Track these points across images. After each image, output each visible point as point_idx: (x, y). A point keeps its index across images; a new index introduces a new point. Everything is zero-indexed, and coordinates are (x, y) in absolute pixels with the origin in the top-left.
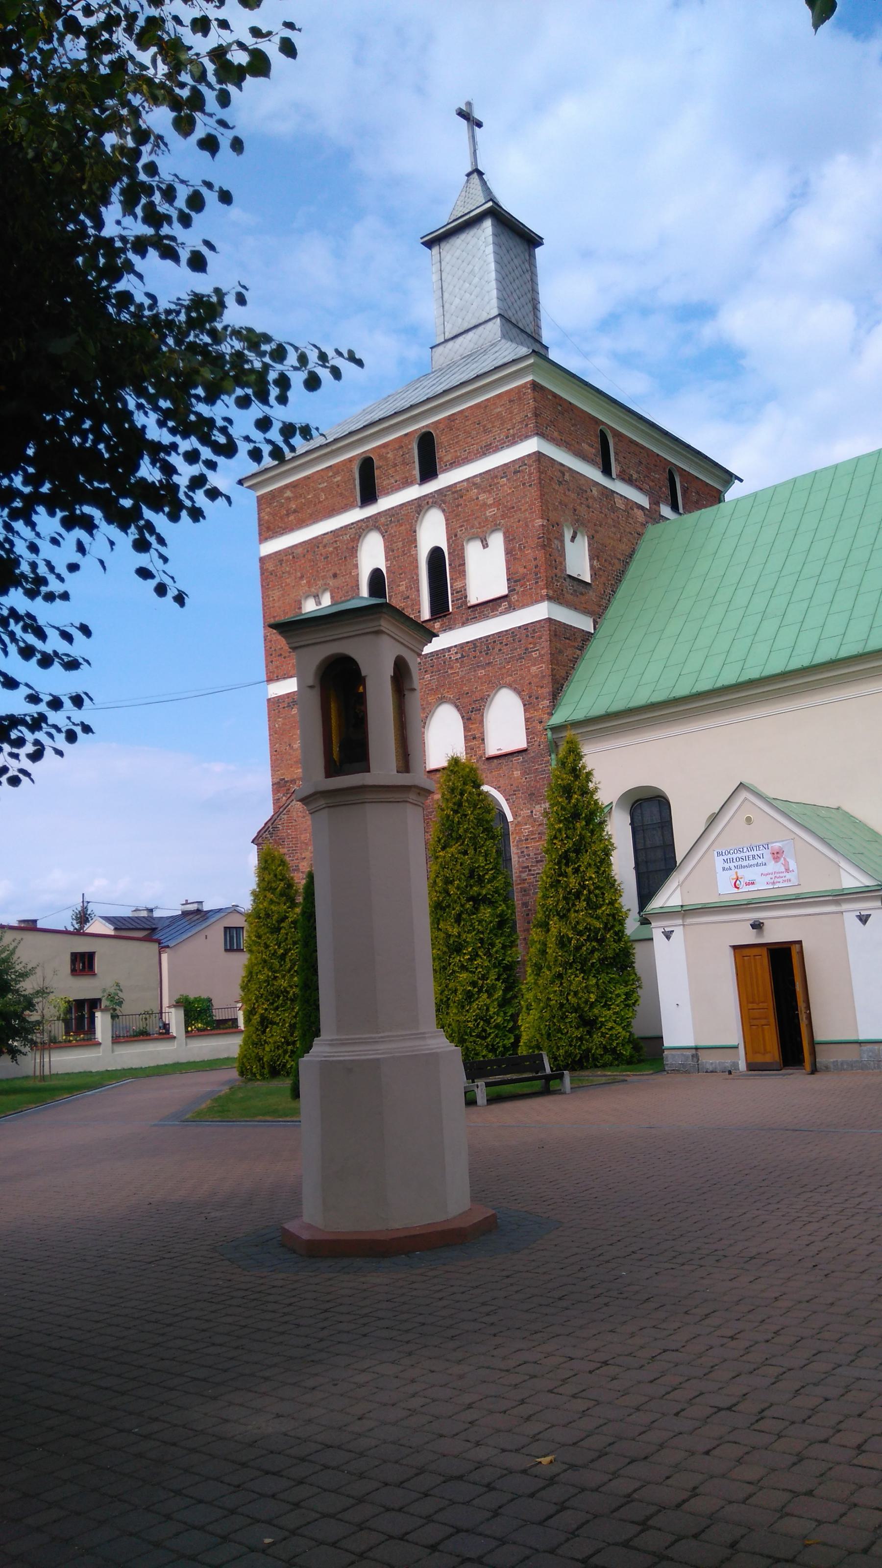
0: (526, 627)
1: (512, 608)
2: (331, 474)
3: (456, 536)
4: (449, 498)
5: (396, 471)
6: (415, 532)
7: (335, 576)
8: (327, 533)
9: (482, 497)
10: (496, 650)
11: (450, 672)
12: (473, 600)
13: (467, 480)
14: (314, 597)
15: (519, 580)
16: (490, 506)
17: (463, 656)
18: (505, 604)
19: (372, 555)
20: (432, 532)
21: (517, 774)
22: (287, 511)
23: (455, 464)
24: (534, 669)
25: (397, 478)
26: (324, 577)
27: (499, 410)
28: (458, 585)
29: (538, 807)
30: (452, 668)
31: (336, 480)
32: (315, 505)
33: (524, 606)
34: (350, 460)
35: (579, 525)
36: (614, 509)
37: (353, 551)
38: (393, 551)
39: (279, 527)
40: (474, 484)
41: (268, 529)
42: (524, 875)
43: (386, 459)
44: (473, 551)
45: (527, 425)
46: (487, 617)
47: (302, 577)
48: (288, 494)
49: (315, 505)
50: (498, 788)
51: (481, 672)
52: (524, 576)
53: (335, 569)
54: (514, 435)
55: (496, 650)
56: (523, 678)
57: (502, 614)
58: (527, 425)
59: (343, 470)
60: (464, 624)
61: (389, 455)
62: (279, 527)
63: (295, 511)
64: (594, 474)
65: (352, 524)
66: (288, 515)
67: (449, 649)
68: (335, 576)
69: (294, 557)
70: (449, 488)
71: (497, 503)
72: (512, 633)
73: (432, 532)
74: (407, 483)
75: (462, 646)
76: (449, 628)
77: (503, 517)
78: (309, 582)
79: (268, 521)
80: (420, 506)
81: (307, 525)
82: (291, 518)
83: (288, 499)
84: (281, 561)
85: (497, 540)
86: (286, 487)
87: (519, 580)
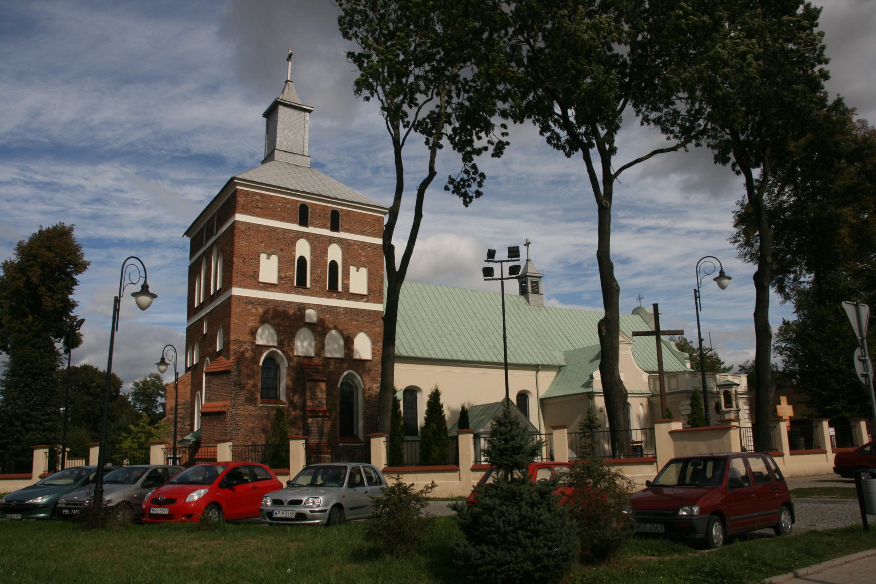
0: (375, 311)
1: (368, 301)
9: (360, 251)
12: (351, 291)
18: (366, 299)
26: (275, 248)
34: (297, 201)
41: (243, 208)
44: (353, 269)
46: (357, 300)
47: (262, 242)
48: (258, 197)
51: (354, 323)
53: (283, 247)
68: (282, 250)
70: (346, 240)
71: (366, 256)
72: (369, 311)
75: (346, 308)
78: (265, 246)
80: (332, 240)
84: (250, 228)
86: (257, 193)
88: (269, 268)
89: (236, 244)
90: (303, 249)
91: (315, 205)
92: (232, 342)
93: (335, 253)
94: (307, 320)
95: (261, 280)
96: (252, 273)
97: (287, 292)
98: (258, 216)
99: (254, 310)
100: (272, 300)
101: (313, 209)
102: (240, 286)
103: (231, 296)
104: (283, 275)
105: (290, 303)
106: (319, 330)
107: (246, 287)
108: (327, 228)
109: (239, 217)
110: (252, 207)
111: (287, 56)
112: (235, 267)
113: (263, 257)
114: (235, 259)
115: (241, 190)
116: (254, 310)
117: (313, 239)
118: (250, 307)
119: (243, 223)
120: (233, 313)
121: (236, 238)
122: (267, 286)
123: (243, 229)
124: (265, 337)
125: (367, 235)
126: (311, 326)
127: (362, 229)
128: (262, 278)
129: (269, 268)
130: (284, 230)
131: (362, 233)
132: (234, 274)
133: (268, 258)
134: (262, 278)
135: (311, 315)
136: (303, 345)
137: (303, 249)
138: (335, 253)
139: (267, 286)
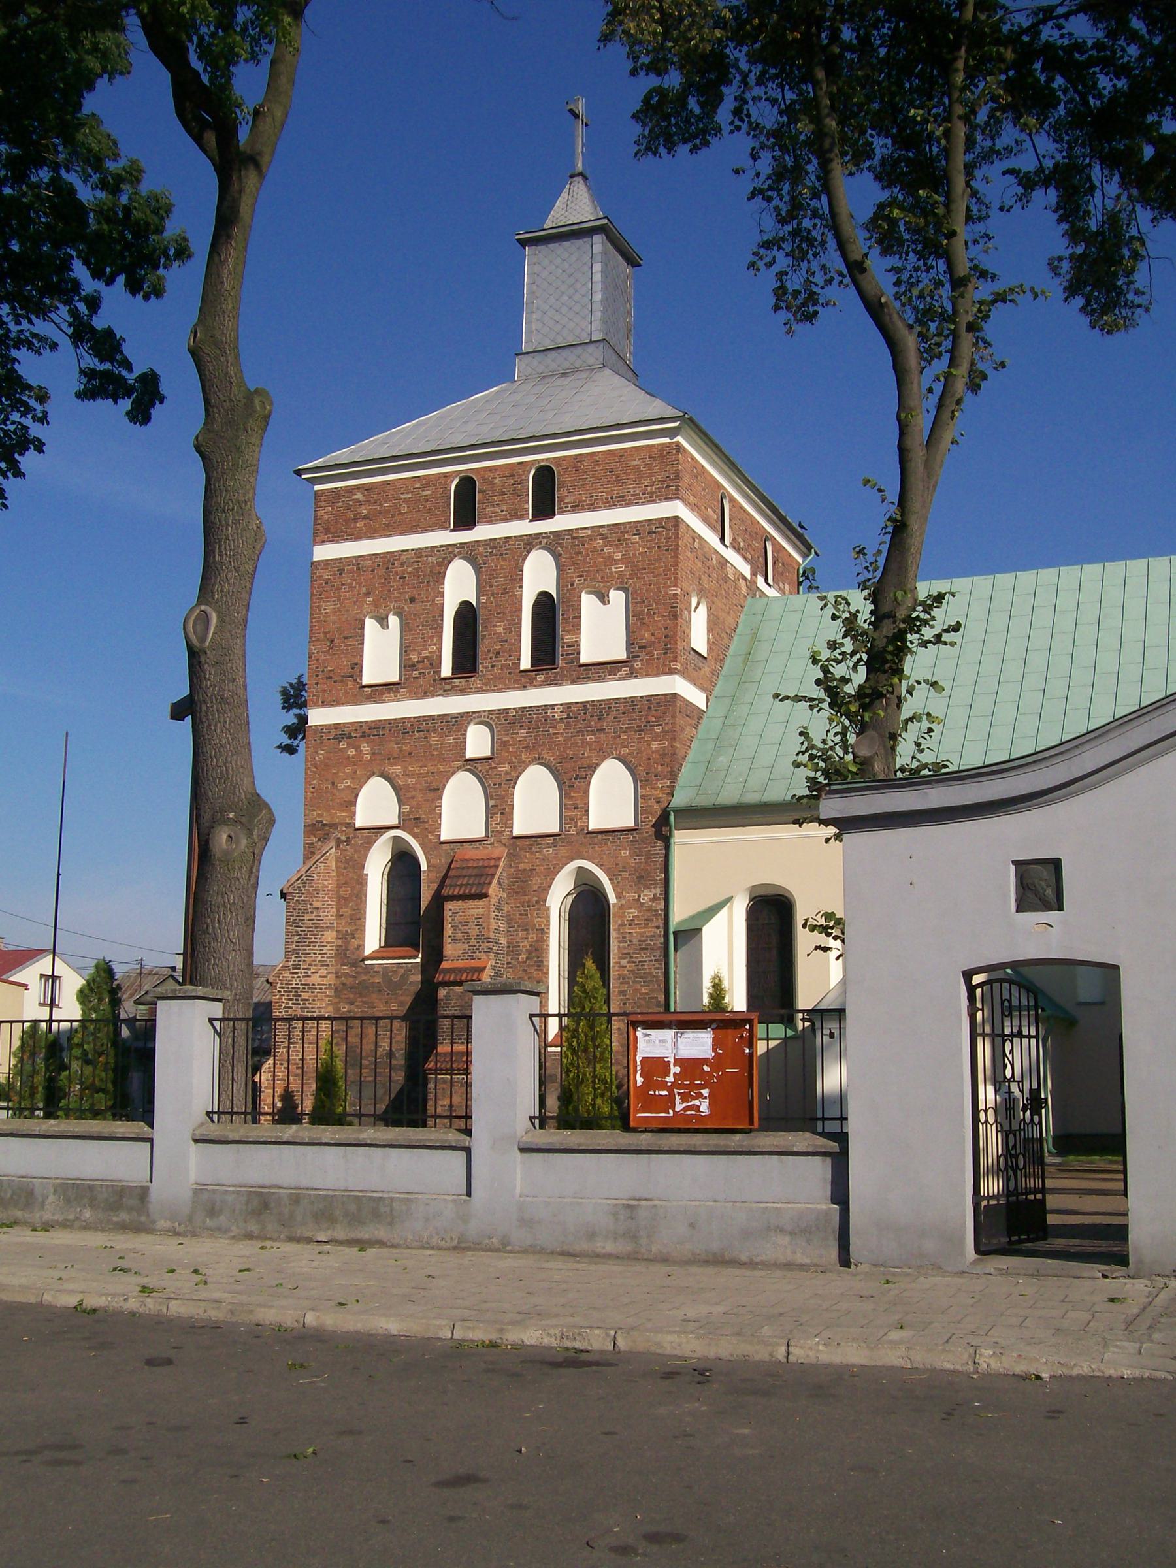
0: (649, 698)
1: (633, 674)
3: (572, 585)
4: (568, 542)
7: (412, 600)
10: (611, 717)
11: (552, 731)
13: (592, 527)
15: (644, 647)
16: (617, 562)
17: (569, 717)
18: (625, 670)
19: (459, 585)
20: (539, 575)
21: (625, 853)
22: (355, 515)
23: (577, 507)
24: (654, 745)
26: (397, 599)
27: (636, 463)
28: (569, 639)
29: (646, 892)
30: (555, 727)
32: (393, 516)
33: (648, 675)
35: (702, 593)
36: (726, 578)
37: (440, 577)
38: (491, 586)
41: (327, 531)
42: (624, 962)
43: (493, 484)
45: (668, 487)
47: (368, 594)
48: (359, 496)
49: (393, 516)
50: (601, 866)
51: (591, 738)
52: (652, 644)
54: (652, 493)
55: (611, 717)
56: (640, 751)
57: (620, 679)
58: (668, 487)
59: (434, 485)
60: (573, 682)
61: (496, 481)
63: (365, 517)
64: (712, 538)
66: (356, 520)
67: (553, 706)
68: (412, 600)
69: (358, 569)
73: (539, 575)
74: (516, 515)
76: (555, 682)
77: (631, 576)
79: (327, 522)
81: (381, 537)
82: (360, 524)
83: (358, 501)
84: (341, 571)
85: (617, 597)
87: (644, 647)
91: (490, 469)
95: (365, 681)
96: (347, 670)
97: (426, 694)
98: (359, 538)
99: (352, 752)
100: (389, 721)
101: (485, 480)
102: (324, 704)
104: (414, 657)
105: (432, 718)
107: (336, 702)
110: (347, 521)
113: (370, 625)
116: (352, 752)
118: (343, 745)
119: (326, 563)
122: (380, 692)
127: (618, 491)
128: (369, 677)
129: (380, 651)
130: (417, 552)
134: (369, 677)
136: (461, 811)
139: (380, 692)
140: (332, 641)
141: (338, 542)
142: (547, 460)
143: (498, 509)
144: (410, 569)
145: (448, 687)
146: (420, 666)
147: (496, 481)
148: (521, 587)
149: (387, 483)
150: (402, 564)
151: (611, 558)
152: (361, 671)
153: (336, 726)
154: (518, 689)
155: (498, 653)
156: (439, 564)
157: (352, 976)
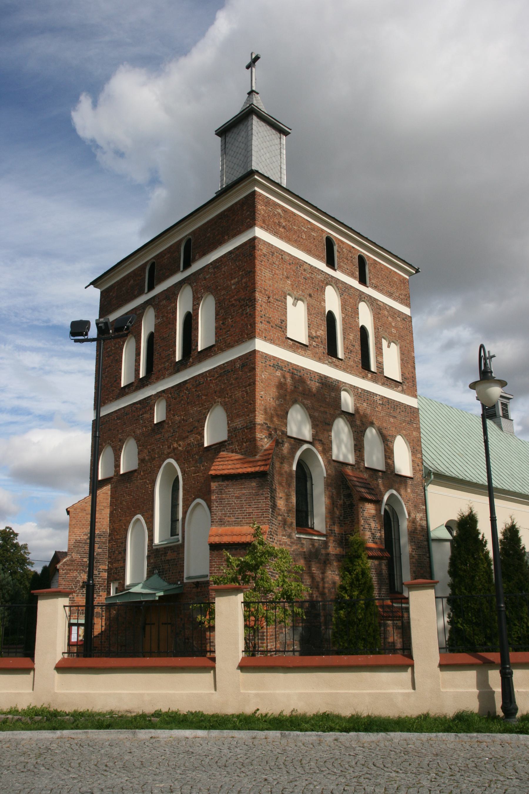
1: (403, 391)
2: (309, 226)
5: (347, 263)
6: (358, 308)
8: (307, 263)
9: (390, 319)
14: (295, 299)
22: (279, 222)
23: (376, 288)
25: (348, 268)
31: (313, 234)
34: (322, 230)
38: (346, 310)
39: (271, 227)
40: (386, 308)
47: (287, 278)
51: (392, 420)
62: (271, 227)
65: (322, 271)
67: (376, 395)
75: (383, 398)
83: (279, 214)
88: (297, 321)
89: (258, 272)
90: (332, 301)
92: (258, 427)
93: (365, 317)
94: (344, 409)
96: (278, 322)
103: (255, 351)
104: (314, 334)
106: (358, 423)
108: (355, 278)
109: (259, 232)
111: (249, 61)
112: (258, 308)
113: (290, 300)
114: (258, 295)
115: (261, 195)
117: (343, 290)
120: (258, 379)
121: (257, 262)
122: (296, 346)
123: (264, 251)
124: (299, 424)
125: (394, 299)
126: (350, 417)
131: (390, 295)
132: (258, 319)
133: (294, 304)
135: (348, 401)
137: (332, 301)
138: (365, 317)
140: (269, 298)
141: (270, 233)
142: (364, 253)
143: (345, 266)
144: (308, 275)
145: (330, 360)
146: (316, 340)
147: (344, 250)
148: (358, 318)
149: (294, 214)
150: (305, 270)
151: (390, 323)
152: (286, 327)
153: (275, 358)
154: (359, 377)
155: (351, 351)
156: (322, 282)
157: (289, 545)
